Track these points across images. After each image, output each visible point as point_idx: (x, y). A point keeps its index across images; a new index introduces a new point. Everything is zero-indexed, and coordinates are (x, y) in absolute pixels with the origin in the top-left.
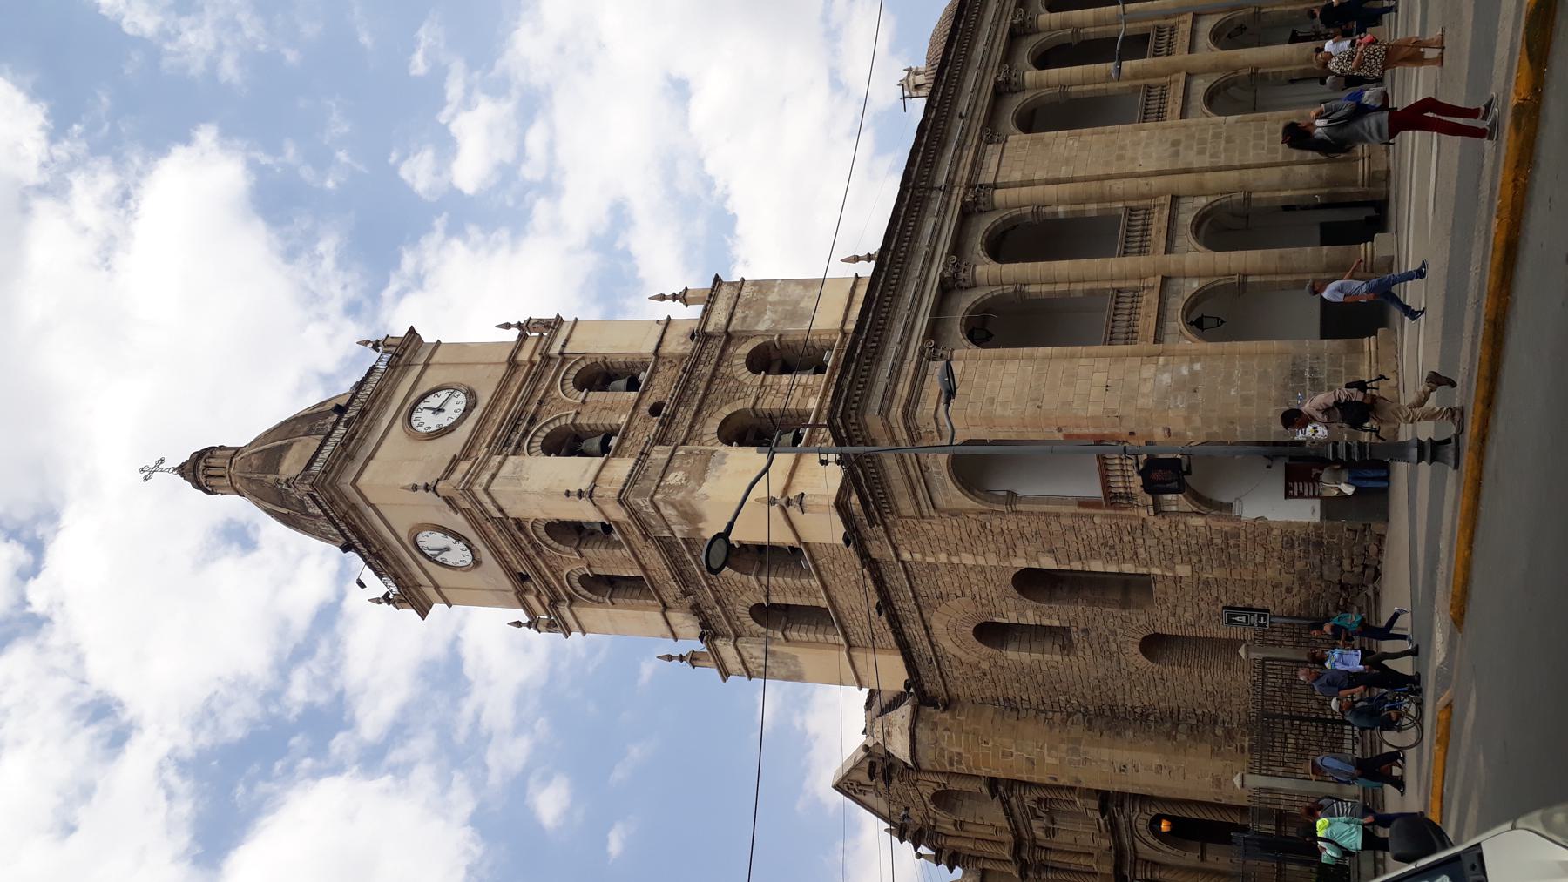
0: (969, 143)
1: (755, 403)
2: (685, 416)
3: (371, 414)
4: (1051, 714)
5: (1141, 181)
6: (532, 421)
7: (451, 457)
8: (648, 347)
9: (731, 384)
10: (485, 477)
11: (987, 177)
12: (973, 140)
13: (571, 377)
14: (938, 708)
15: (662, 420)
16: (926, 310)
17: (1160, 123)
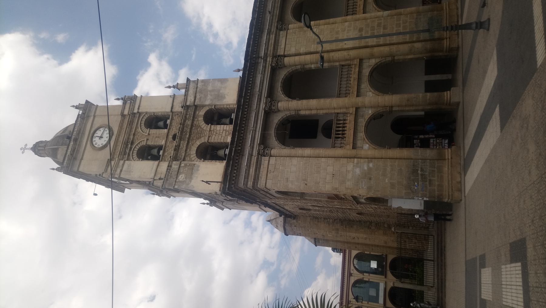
0: (272, 30)
1: (208, 139)
2: (184, 144)
3: (79, 140)
4: (329, 220)
5: (345, 53)
6: (132, 143)
7: (107, 160)
8: (168, 109)
9: (199, 129)
10: (119, 171)
11: (281, 52)
12: (274, 29)
13: (143, 122)
14: (291, 218)
15: (175, 148)
16: (260, 128)
17: (354, 16)
